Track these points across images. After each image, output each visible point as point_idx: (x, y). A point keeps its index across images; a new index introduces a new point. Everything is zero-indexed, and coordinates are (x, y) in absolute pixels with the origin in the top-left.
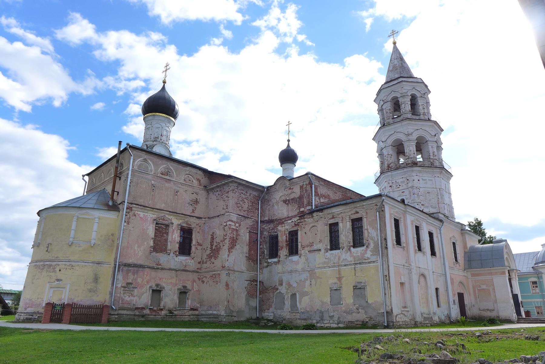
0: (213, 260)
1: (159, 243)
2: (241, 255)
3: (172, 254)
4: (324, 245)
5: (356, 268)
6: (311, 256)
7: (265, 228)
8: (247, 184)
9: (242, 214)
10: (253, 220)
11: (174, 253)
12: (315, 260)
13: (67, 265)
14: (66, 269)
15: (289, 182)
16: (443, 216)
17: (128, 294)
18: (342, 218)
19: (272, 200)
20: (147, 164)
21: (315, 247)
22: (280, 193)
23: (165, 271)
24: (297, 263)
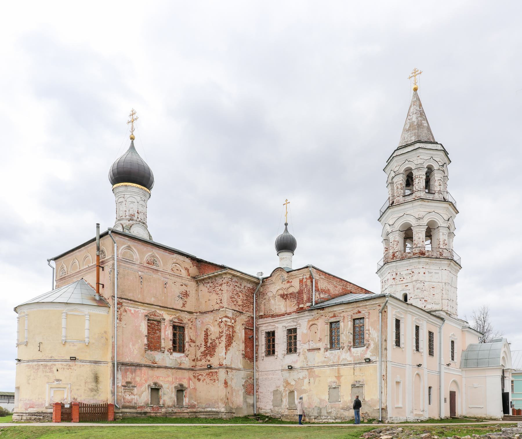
0: (208, 357)
1: (153, 341)
2: (237, 353)
3: (166, 352)
4: (324, 344)
5: (355, 368)
8: (241, 276)
9: (237, 310)
10: (248, 315)
11: (168, 351)
12: (314, 359)
13: (64, 364)
14: (64, 369)
15: (288, 274)
16: (445, 314)
18: (344, 317)
19: (268, 294)
22: (277, 286)
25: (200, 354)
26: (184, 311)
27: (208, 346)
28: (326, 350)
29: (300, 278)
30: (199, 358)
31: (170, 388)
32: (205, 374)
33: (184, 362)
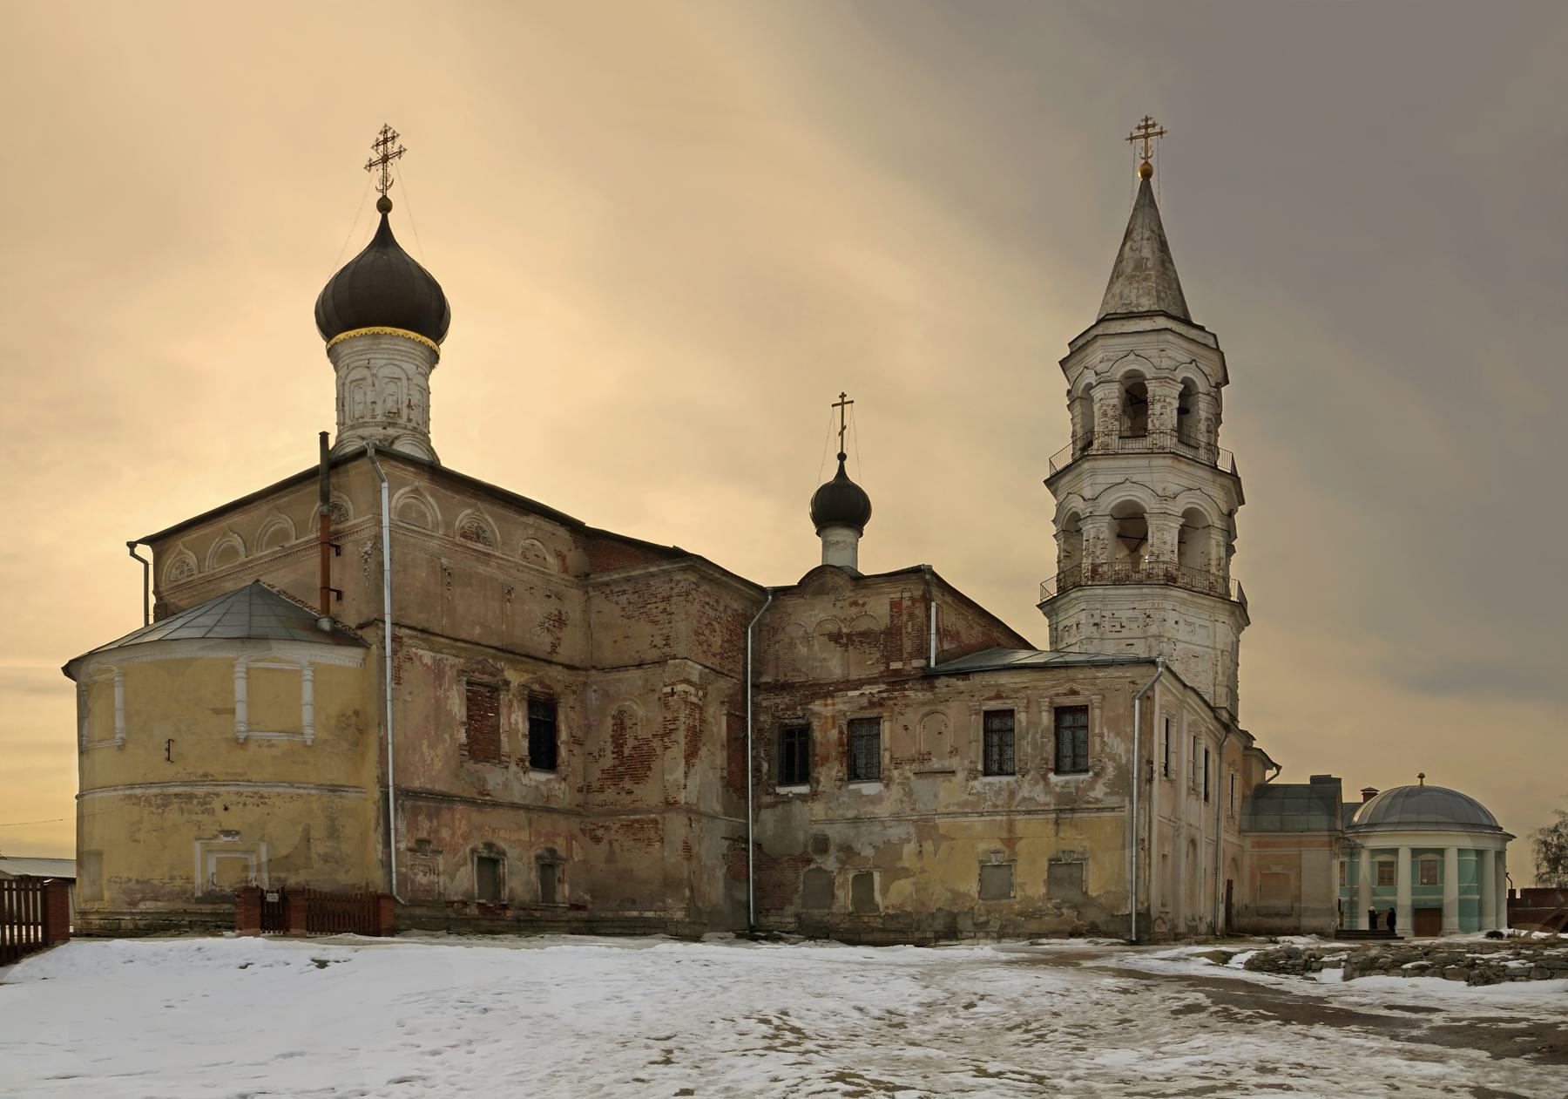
3: (513, 767)
9: (709, 665)
11: (518, 765)
19: (788, 629)
22: (817, 611)
25: (598, 774)
27: (625, 755)
31: (525, 858)
33: (557, 793)
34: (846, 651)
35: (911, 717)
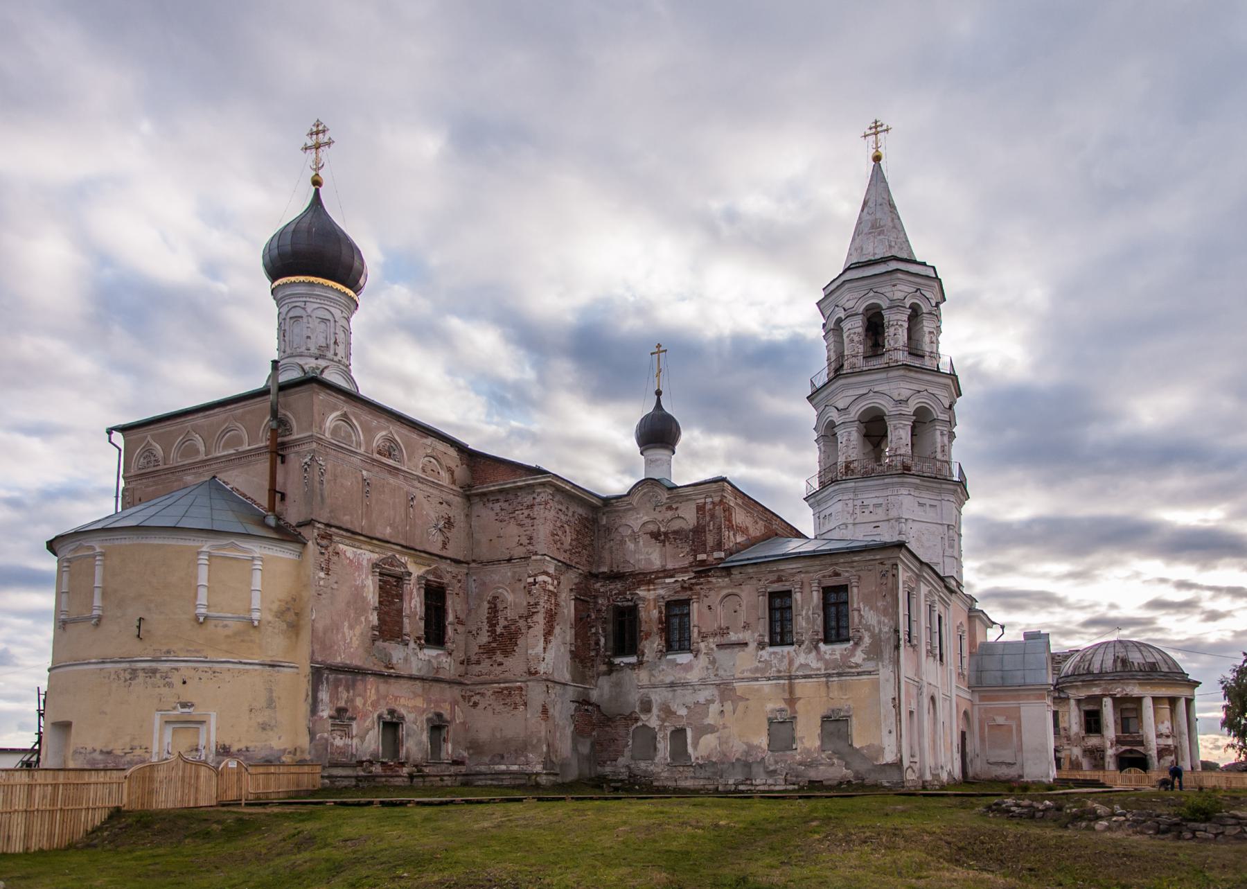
0: (499, 657)
1: (388, 619)
3: (412, 645)
4: (756, 635)
6: (723, 656)
7: (601, 590)
8: (573, 490)
9: (562, 559)
10: (580, 571)
11: (415, 642)
15: (669, 492)
17: (339, 733)
19: (620, 530)
20: (350, 428)
21: (733, 637)
23: (402, 681)
24: (688, 668)
25: (476, 649)
26: (446, 558)
28: (761, 646)
29: (698, 501)
30: (474, 658)
32: (491, 692)
33: (444, 665)
34: (664, 546)
35: (714, 598)
